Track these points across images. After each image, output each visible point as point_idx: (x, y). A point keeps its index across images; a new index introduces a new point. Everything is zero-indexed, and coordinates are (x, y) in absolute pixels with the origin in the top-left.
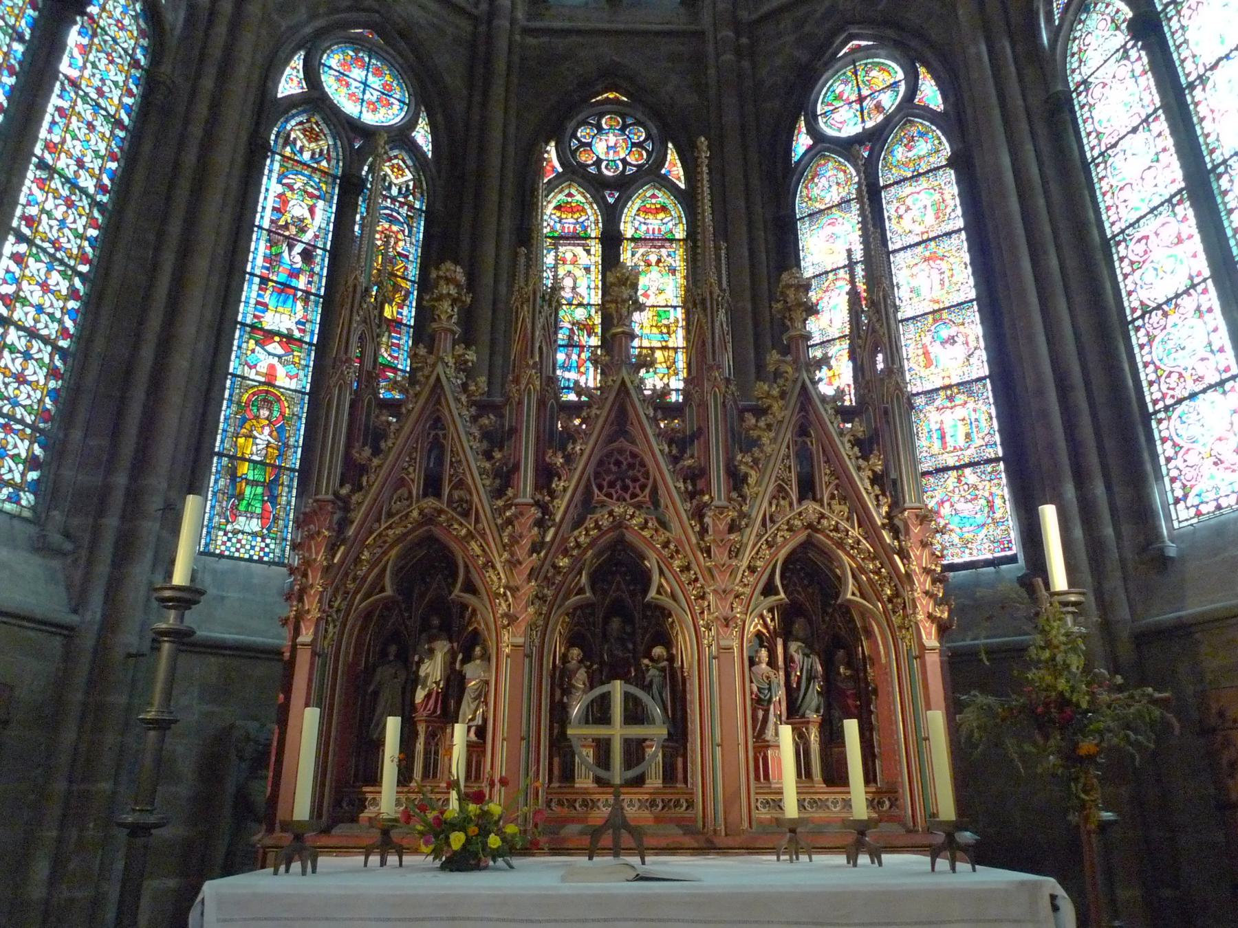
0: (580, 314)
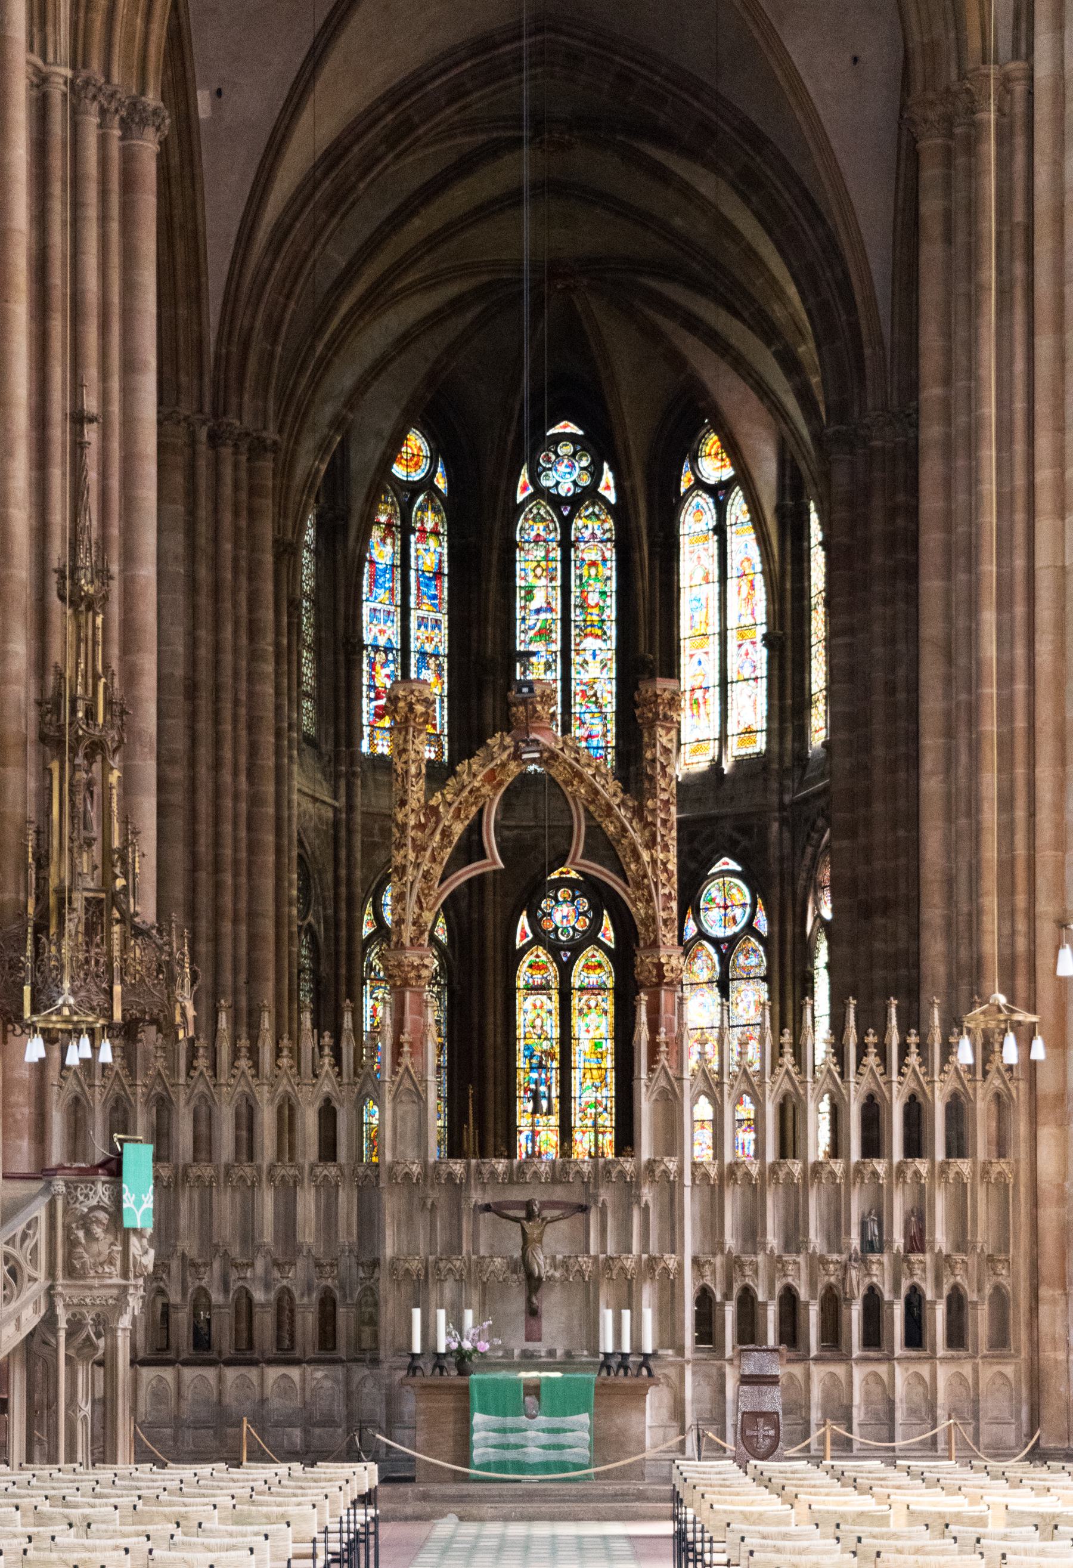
0: (546, 1045)
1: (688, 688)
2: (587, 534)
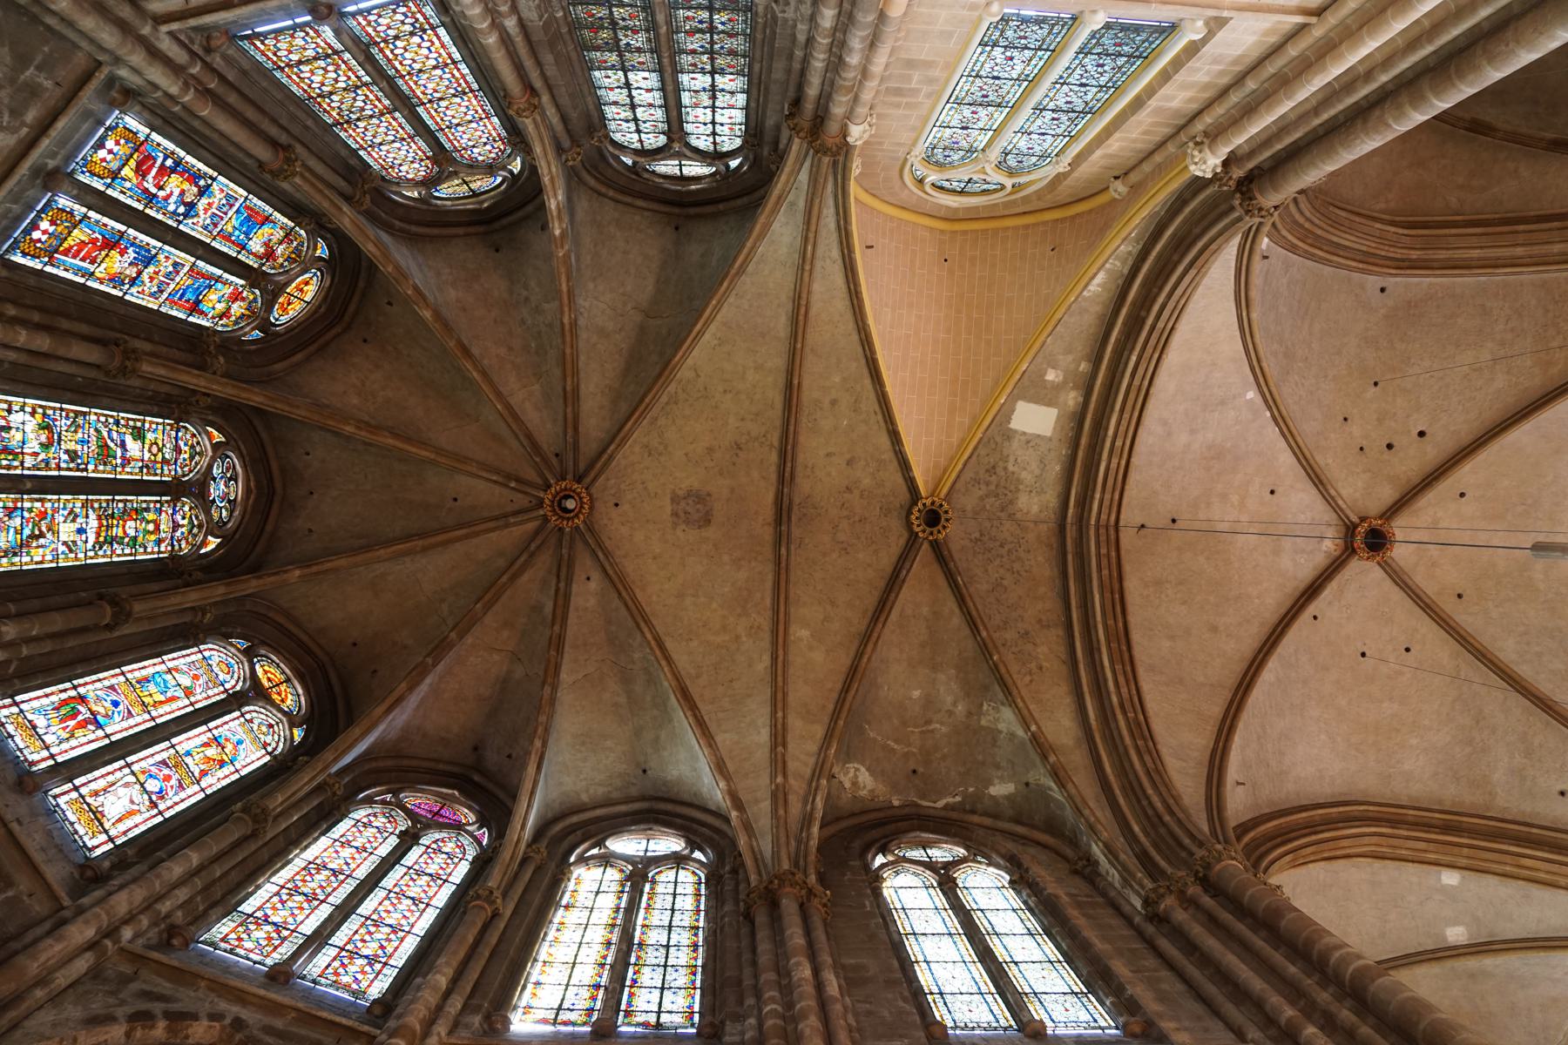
1: (82, 690)
2: (178, 517)
